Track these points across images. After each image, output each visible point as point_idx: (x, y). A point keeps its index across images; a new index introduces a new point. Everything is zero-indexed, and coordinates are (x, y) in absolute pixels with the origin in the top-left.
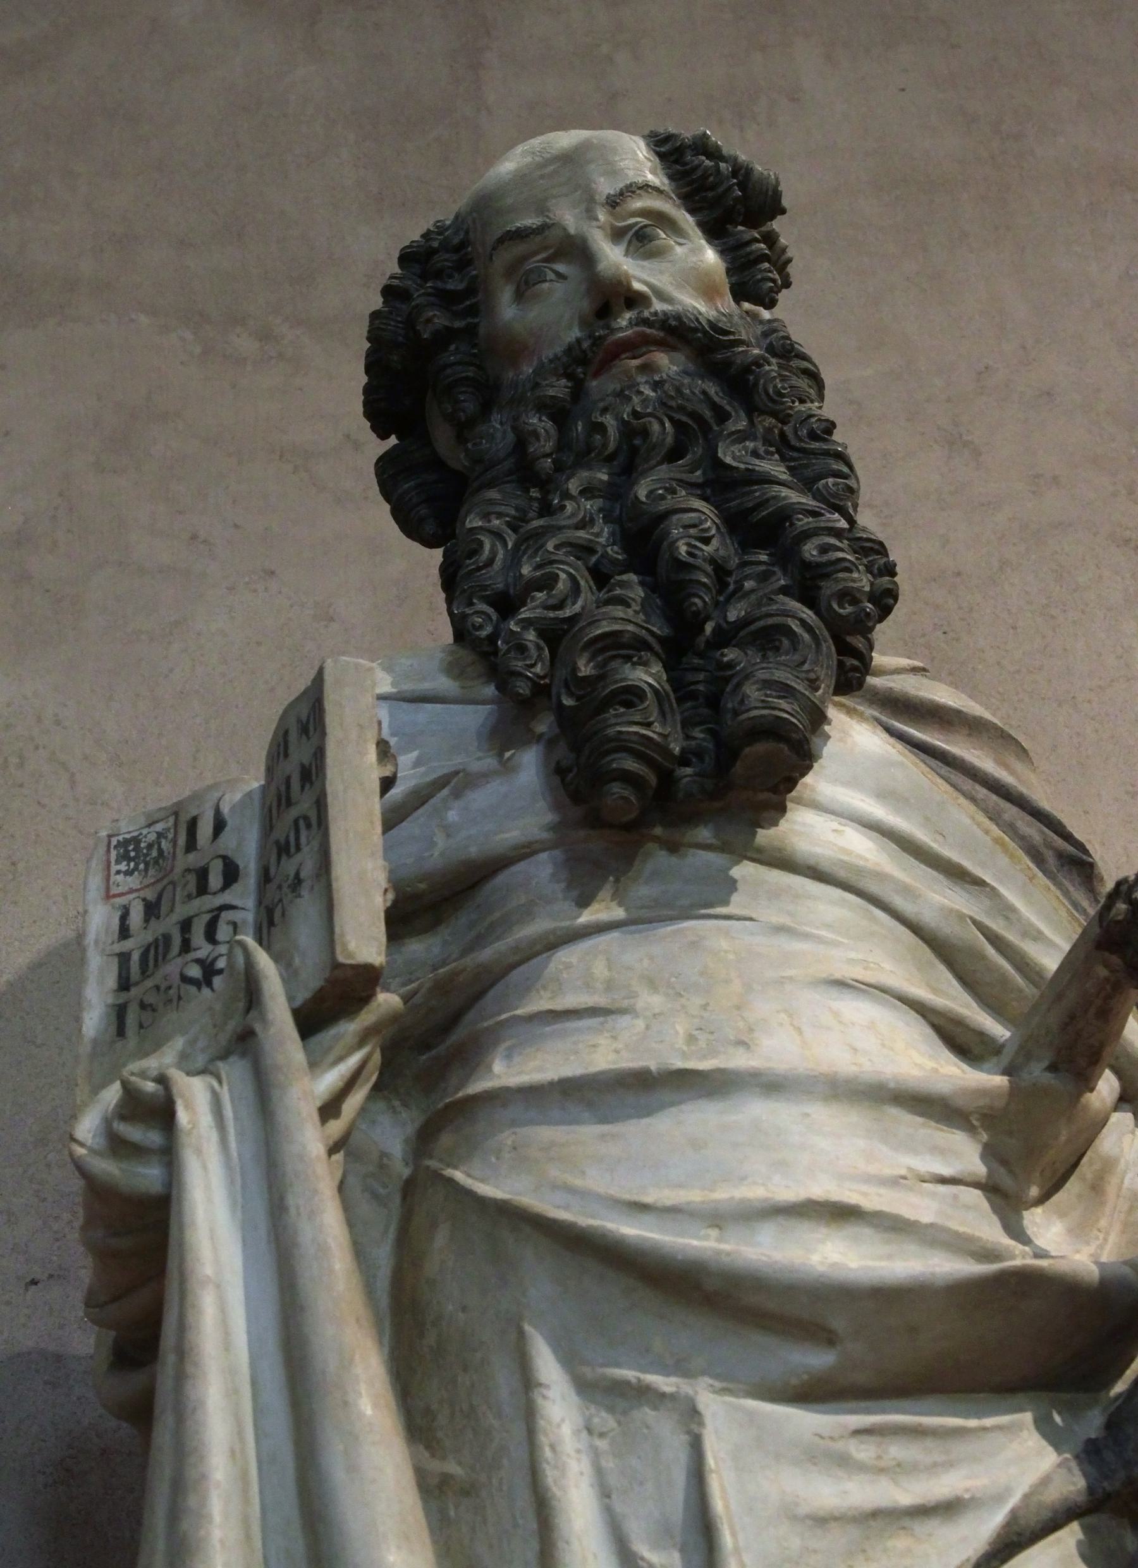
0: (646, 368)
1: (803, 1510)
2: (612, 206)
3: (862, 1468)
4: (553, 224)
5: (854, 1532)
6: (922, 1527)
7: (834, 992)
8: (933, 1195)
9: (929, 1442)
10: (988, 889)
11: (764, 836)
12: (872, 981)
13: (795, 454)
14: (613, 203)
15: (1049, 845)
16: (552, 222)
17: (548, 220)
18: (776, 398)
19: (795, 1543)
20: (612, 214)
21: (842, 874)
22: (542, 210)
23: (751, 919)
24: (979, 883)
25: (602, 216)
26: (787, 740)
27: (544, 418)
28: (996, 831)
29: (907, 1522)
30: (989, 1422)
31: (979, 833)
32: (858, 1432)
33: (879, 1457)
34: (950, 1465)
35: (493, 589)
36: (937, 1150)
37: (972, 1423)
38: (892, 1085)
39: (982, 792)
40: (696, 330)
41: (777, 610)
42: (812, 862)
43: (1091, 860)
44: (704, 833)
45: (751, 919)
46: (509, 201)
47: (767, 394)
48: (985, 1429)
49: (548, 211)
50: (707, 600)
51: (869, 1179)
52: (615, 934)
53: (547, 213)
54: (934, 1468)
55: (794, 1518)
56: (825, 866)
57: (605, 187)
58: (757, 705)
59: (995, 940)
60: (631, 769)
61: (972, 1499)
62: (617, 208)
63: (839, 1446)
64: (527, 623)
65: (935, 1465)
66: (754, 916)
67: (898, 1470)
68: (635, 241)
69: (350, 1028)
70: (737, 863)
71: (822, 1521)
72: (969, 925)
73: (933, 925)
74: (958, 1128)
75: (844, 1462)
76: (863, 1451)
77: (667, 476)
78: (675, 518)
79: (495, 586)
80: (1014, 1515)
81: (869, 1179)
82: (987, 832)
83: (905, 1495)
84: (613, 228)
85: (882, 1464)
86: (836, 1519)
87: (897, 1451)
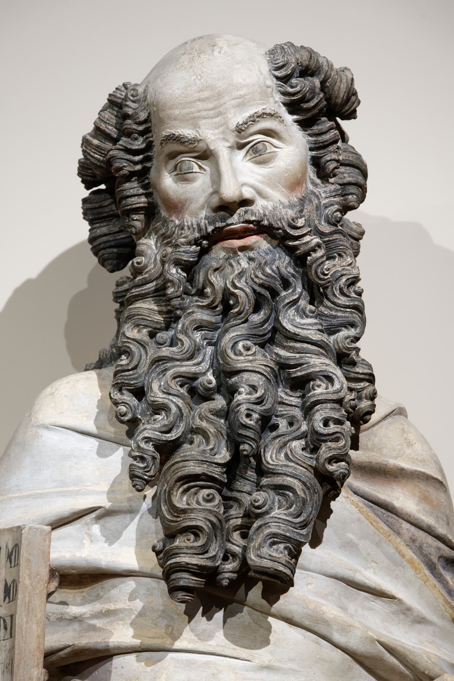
2: (238, 132)
4: (201, 140)
10: (396, 600)
13: (329, 304)
16: (200, 138)
17: (198, 135)
18: (322, 276)
20: (237, 136)
21: (307, 623)
22: (196, 126)
24: (392, 597)
27: (180, 271)
35: (135, 386)
40: (278, 229)
41: (291, 473)
46: (177, 112)
47: (316, 272)
49: (199, 128)
50: (254, 447)
53: (198, 130)
58: (266, 557)
59: (391, 650)
60: (191, 585)
62: (242, 133)
64: (148, 440)
68: (251, 152)
72: (376, 644)
73: (355, 647)
77: (246, 333)
78: (246, 376)
79: (136, 385)
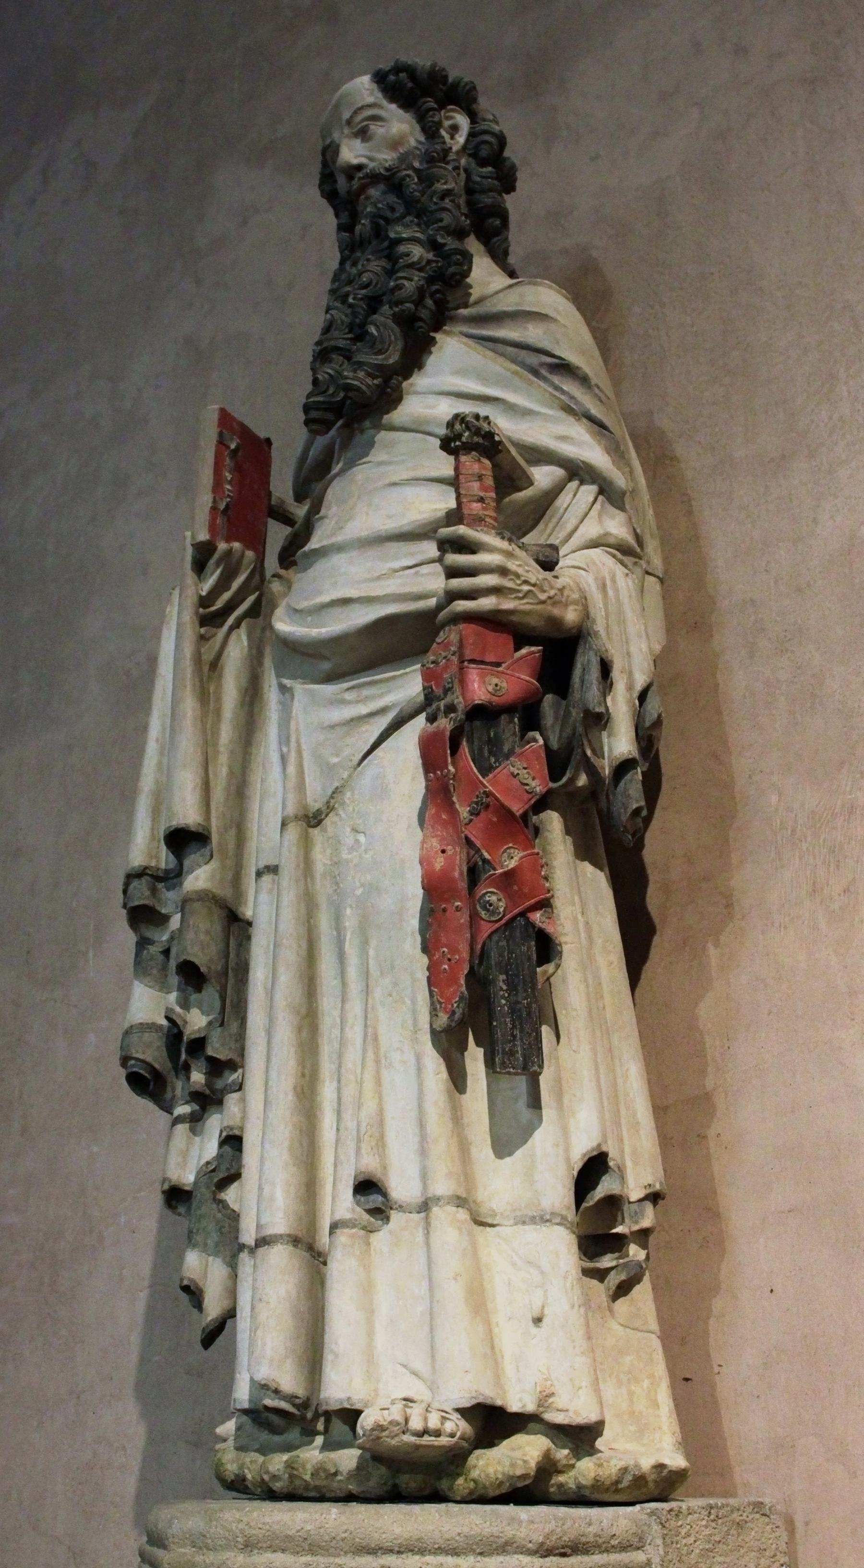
0: (368, 198)
1: (325, 725)
3: (350, 702)
5: (345, 728)
6: (372, 720)
7: (393, 489)
8: (401, 577)
9: (379, 686)
11: (386, 418)
12: (410, 478)
14: (349, 122)
15: (542, 364)
19: (322, 737)
21: (413, 427)
23: (370, 462)
25: (346, 131)
26: (355, 390)
28: (514, 367)
29: (367, 720)
30: (408, 670)
31: (503, 371)
32: (348, 689)
33: (359, 696)
34: (389, 692)
36: (412, 554)
37: (402, 671)
38: (384, 534)
39: (510, 349)
42: (401, 425)
43: (566, 362)
44: (367, 424)
45: (370, 462)
48: (406, 673)
51: (366, 581)
52: (338, 478)
54: (381, 695)
55: (323, 728)
56: (407, 425)
57: (346, 115)
61: (393, 705)
63: (339, 696)
65: (382, 693)
66: (372, 460)
67: (367, 699)
69: (212, 562)
70: (378, 432)
71: (333, 727)
74: (424, 540)
75: (343, 702)
76: (348, 696)
80: (401, 711)
81: (366, 581)
82: (509, 370)
83: (364, 710)
84: (353, 133)
85: (359, 699)
86: (337, 725)
87: (366, 692)
